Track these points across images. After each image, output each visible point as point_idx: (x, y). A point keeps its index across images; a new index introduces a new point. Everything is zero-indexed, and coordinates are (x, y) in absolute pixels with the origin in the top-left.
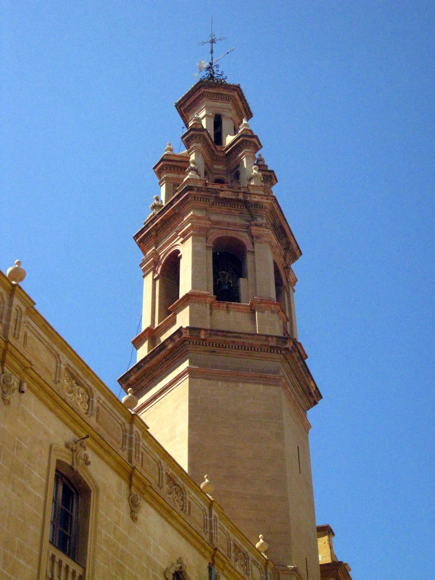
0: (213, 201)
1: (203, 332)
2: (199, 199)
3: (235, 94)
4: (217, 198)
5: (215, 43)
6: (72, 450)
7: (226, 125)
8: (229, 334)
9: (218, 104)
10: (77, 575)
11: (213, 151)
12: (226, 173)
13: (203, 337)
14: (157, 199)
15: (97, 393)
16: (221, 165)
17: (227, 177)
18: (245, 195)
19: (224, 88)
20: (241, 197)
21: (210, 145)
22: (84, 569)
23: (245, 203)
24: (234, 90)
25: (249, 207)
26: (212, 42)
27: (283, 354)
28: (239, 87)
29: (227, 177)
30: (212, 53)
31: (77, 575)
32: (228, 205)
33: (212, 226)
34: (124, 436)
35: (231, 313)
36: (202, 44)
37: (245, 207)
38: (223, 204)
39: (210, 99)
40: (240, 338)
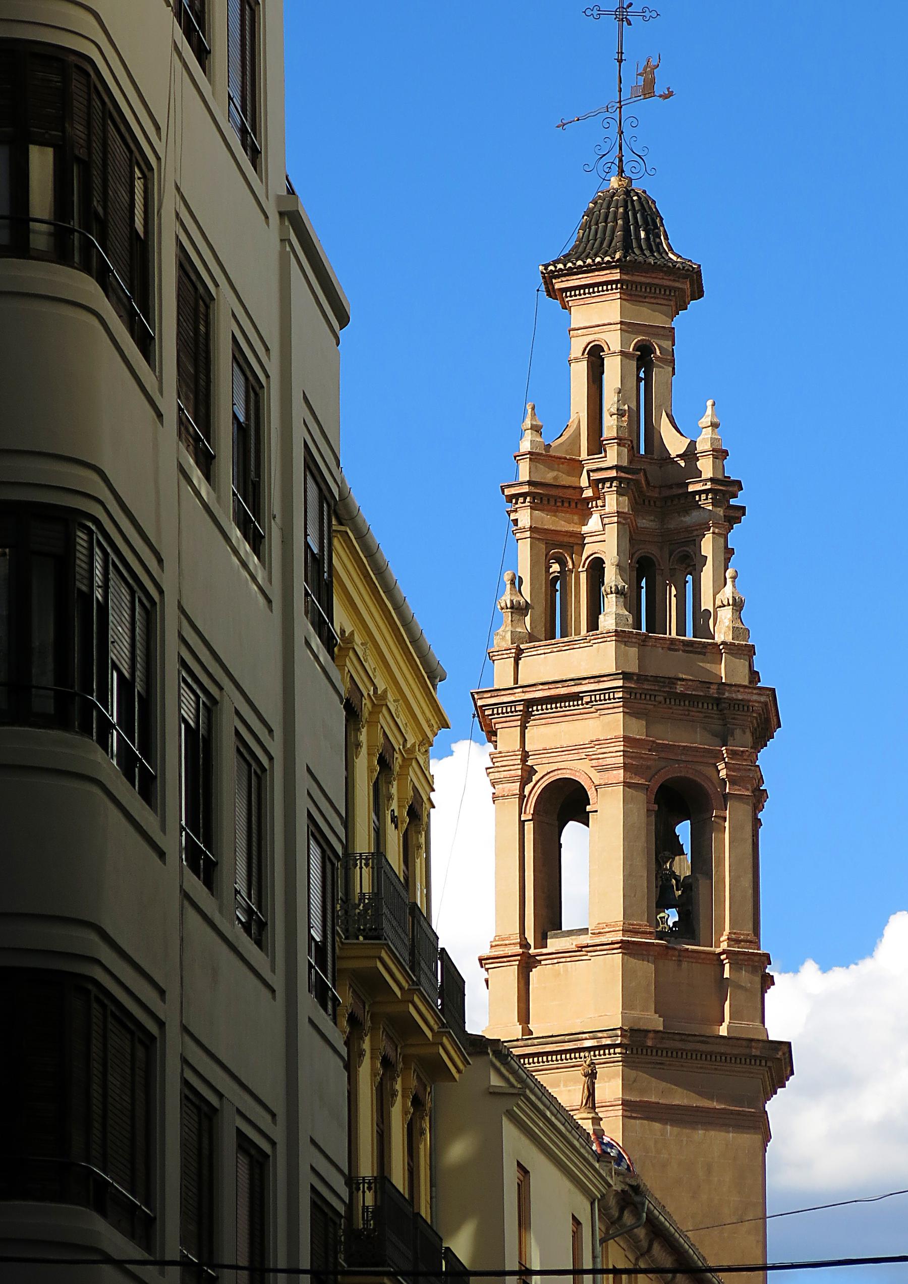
1: (651, 1035)
5: (629, 24)
8: (690, 1038)
13: (650, 1043)
14: (516, 582)
19: (665, 273)
20: (713, 691)
23: (718, 701)
24: (685, 277)
26: (622, 15)
27: (770, 1068)
30: (620, 61)
32: (687, 703)
35: (685, 965)
36: (595, 12)
37: (715, 708)
39: (631, 295)
40: (707, 1043)
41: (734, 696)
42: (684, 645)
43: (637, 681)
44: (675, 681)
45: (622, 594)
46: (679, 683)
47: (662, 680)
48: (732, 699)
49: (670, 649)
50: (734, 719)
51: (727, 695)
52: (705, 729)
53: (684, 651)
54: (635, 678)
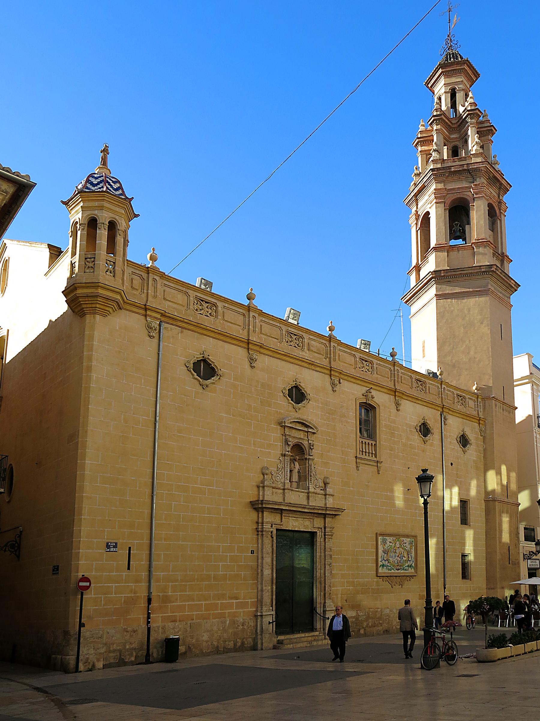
0: (447, 175)
2: (439, 176)
3: (466, 67)
4: (450, 172)
6: (365, 396)
7: (459, 96)
9: (453, 80)
10: (373, 444)
11: (449, 126)
12: (459, 139)
15: (375, 361)
16: (455, 133)
17: (460, 142)
18: (468, 165)
21: (447, 123)
22: (376, 442)
23: (468, 170)
25: (472, 172)
28: (467, 60)
29: (460, 142)
31: (373, 444)
32: (458, 175)
33: (448, 193)
34: (391, 374)
37: (468, 173)
38: (454, 175)
41: (473, 167)
42: (458, 159)
43: (437, 170)
44: (450, 167)
45: (436, 151)
46: (452, 168)
47: (446, 168)
48: (473, 168)
49: (453, 162)
50: (476, 175)
51: (470, 167)
52: (466, 182)
53: (459, 161)
54: (436, 170)
